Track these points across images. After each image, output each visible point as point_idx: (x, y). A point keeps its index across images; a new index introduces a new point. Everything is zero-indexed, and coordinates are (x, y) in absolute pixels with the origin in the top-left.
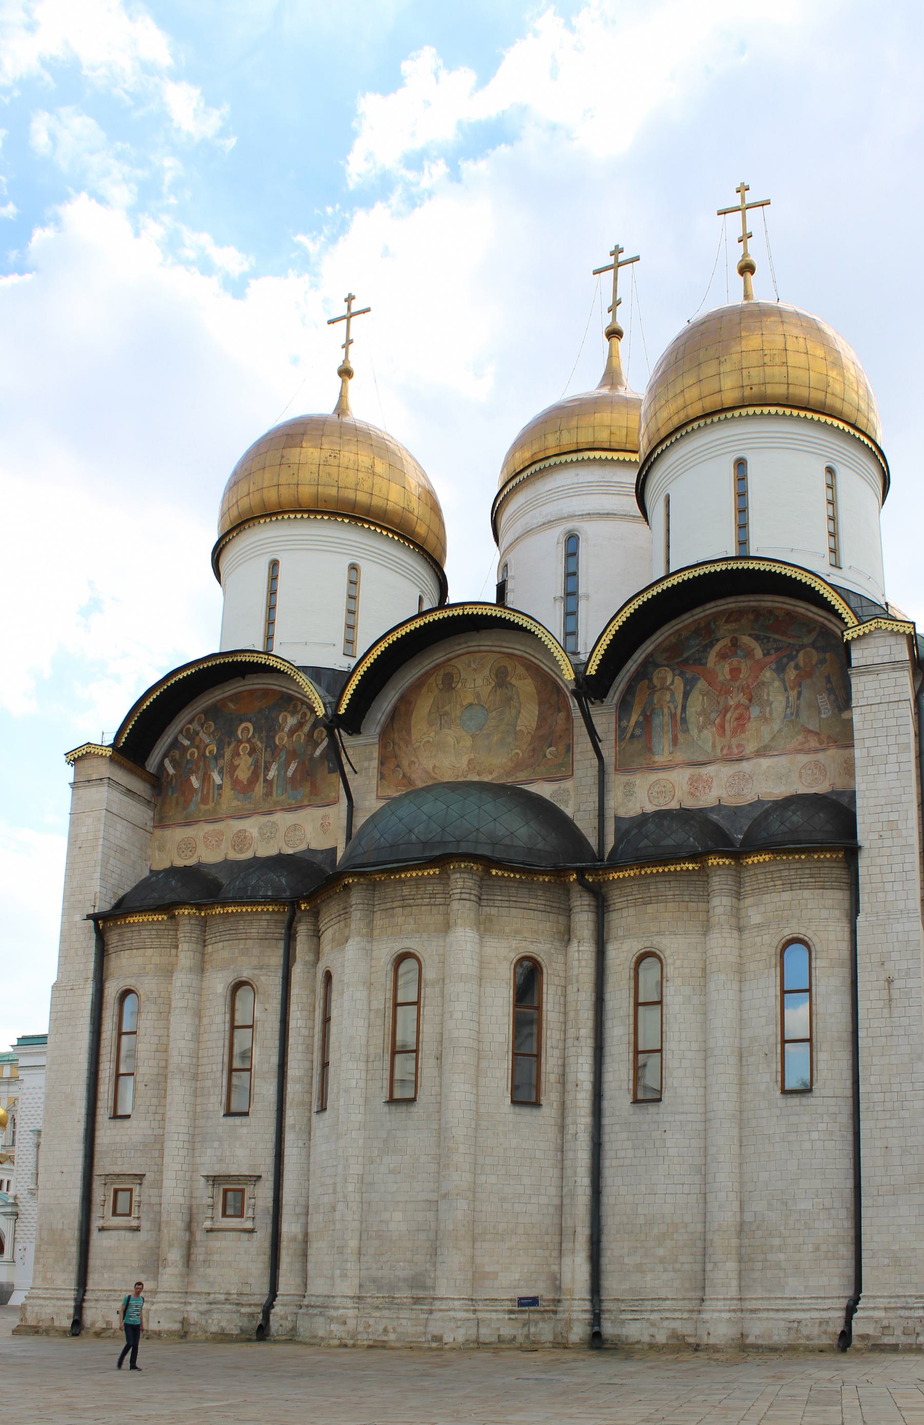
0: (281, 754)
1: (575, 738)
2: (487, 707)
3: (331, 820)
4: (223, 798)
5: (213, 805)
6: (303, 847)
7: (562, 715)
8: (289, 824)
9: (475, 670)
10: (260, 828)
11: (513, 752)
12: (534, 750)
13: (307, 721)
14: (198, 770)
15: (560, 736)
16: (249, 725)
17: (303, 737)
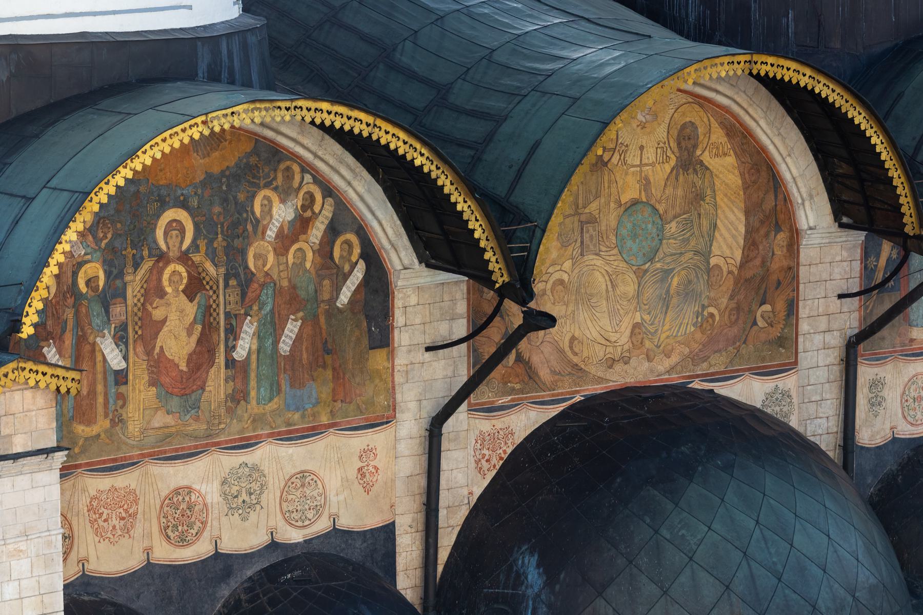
0: (263, 297)
1: (801, 287)
2: (661, 212)
3: (380, 462)
4: (131, 407)
5: (107, 423)
6: (322, 526)
7: (782, 238)
8: (290, 470)
9: (642, 126)
10: (224, 482)
11: (705, 313)
12: (738, 308)
13: (315, 216)
14: (64, 331)
15: (779, 283)
16: (182, 215)
17: (310, 255)
